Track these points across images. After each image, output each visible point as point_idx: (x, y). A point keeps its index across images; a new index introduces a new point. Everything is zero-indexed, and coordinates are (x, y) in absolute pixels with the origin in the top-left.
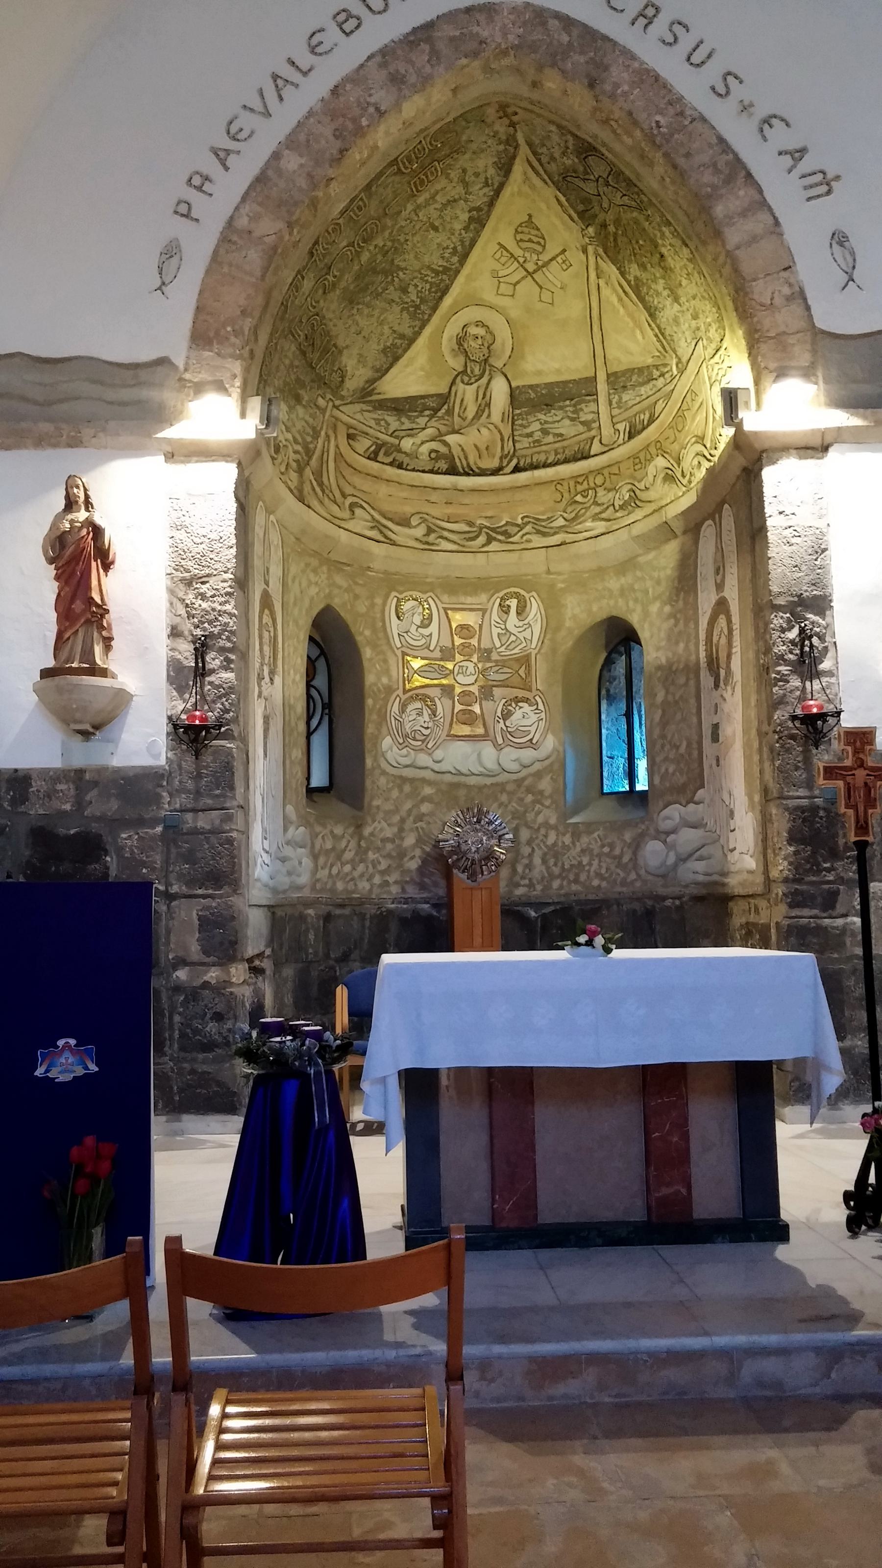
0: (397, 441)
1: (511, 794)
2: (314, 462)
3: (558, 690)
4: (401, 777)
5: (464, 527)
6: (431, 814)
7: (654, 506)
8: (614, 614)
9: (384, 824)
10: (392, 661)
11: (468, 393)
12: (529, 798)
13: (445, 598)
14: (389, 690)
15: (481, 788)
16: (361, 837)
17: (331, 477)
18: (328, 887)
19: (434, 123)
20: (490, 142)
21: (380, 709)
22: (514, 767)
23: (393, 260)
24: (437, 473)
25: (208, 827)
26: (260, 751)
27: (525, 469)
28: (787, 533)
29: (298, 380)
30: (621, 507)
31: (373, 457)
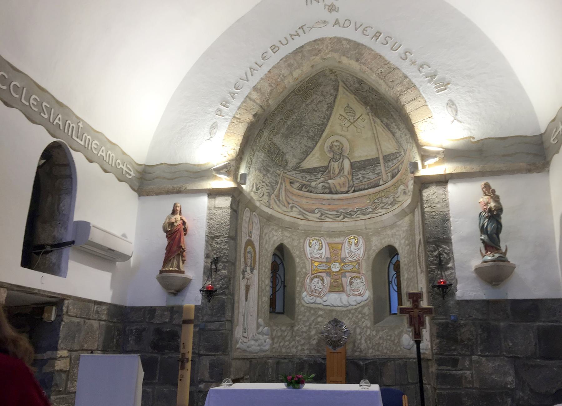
0: (309, 183)
1: (353, 314)
2: (275, 192)
3: (370, 273)
4: (310, 307)
5: (334, 213)
6: (322, 322)
7: (401, 203)
8: (390, 244)
9: (303, 326)
10: (307, 263)
11: (335, 165)
12: (360, 316)
13: (328, 239)
14: (306, 274)
15: (341, 312)
16: (293, 331)
17: (283, 197)
18: (279, 350)
19: (307, 78)
20: (330, 82)
21: (302, 282)
22: (354, 303)
23: (301, 123)
24: (325, 194)
25: (215, 328)
26: (244, 298)
27: (357, 191)
28: (432, 214)
29: (268, 165)
30: (391, 204)
31: (300, 189)
